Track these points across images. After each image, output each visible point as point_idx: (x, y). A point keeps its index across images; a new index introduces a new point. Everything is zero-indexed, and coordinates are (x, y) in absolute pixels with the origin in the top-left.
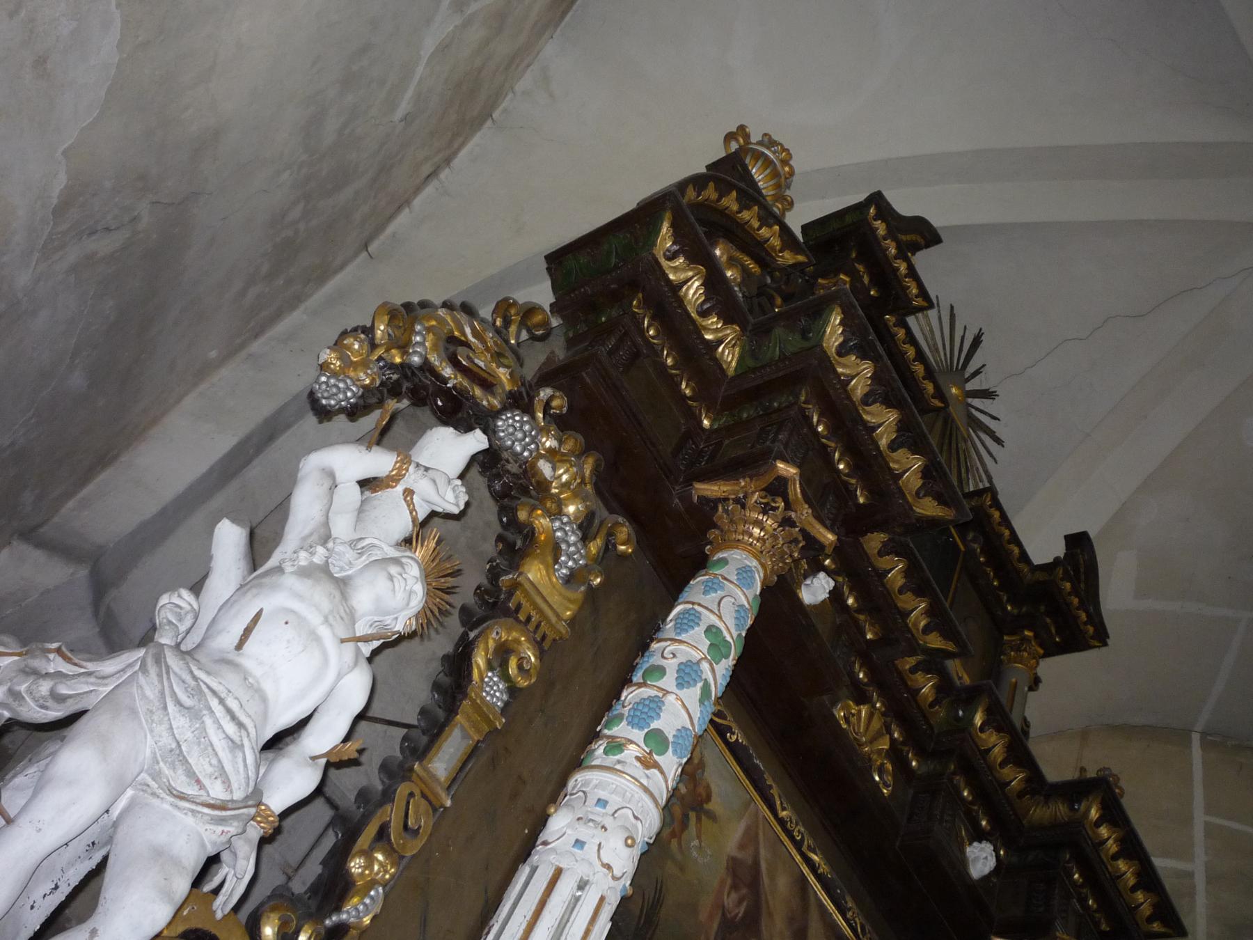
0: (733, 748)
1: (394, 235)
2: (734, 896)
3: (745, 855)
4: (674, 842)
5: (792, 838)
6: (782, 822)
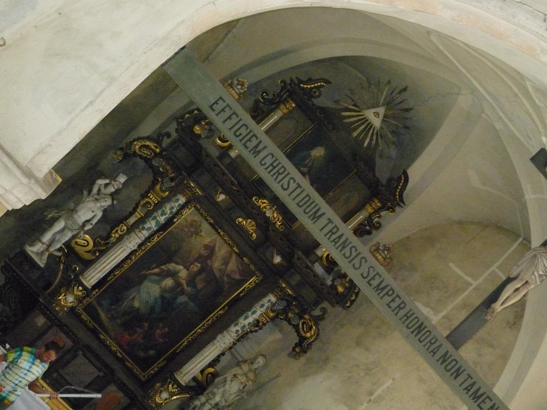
0: (210, 224)
1: (218, 52)
2: (204, 251)
3: (212, 245)
4: (187, 239)
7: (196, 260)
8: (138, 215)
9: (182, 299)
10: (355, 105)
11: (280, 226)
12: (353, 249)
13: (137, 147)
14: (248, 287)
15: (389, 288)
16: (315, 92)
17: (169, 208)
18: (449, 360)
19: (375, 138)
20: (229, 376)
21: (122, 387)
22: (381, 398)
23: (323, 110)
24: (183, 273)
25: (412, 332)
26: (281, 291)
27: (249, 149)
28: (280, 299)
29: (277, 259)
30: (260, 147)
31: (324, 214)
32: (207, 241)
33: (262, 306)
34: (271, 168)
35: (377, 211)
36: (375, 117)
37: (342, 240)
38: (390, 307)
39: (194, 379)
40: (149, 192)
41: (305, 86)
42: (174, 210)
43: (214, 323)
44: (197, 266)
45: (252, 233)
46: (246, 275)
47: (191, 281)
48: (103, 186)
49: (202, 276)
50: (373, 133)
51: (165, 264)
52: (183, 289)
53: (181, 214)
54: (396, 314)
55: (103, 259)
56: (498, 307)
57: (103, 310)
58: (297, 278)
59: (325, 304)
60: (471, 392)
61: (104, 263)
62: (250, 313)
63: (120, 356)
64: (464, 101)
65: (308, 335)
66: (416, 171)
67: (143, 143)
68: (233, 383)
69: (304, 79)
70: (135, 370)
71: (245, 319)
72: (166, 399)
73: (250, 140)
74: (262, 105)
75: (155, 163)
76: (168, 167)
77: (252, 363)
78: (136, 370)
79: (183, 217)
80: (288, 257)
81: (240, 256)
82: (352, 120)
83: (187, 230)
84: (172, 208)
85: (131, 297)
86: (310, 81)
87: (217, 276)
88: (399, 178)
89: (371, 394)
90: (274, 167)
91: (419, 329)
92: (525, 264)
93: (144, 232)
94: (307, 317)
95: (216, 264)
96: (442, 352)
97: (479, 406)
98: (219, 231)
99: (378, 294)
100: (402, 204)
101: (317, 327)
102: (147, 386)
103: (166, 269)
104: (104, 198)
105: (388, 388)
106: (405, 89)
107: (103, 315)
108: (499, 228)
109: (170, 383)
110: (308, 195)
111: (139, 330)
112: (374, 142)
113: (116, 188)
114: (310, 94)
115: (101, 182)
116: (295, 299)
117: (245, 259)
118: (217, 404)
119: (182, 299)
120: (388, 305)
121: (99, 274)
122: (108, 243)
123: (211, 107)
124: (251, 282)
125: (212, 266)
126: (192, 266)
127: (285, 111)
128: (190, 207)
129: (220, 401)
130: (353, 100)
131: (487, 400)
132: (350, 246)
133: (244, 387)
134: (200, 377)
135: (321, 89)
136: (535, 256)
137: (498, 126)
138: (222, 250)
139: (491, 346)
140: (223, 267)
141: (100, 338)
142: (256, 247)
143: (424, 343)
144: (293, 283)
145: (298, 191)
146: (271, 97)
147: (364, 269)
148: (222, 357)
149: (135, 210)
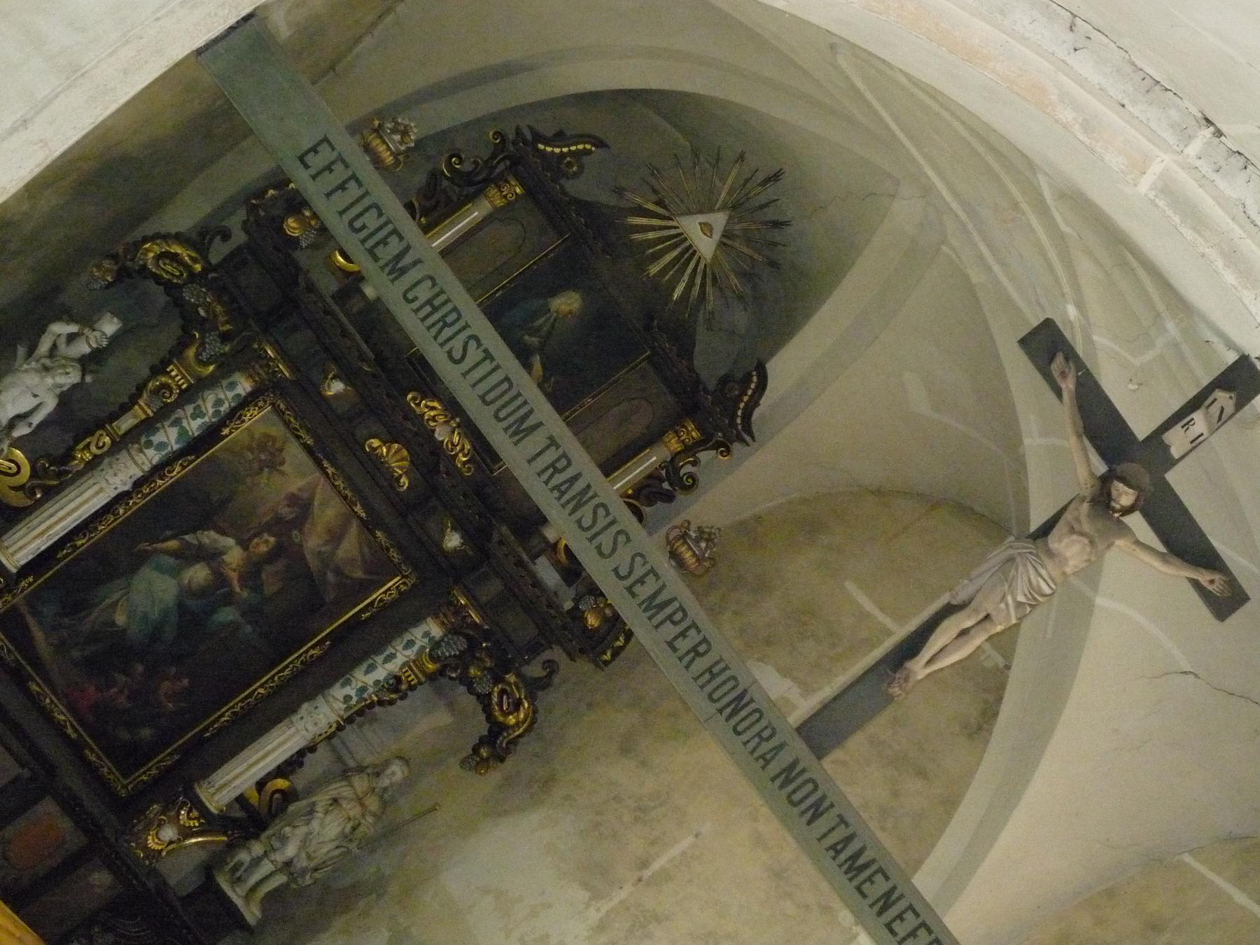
0: (306, 447)
2: (287, 510)
3: (305, 495)
4: (248, 480)
7: (268, 528)
8: (140, 412)
9: (227, 615)
10: (659, 203)
11: (464, 463)
12: (601, 512)
13: (151, 255)
14: (381, 600)
15: (676, 604)
16: (569, 165)
17: (212, 404)
18: (799, 781)
19: (698, 280)
20: (322, 799)
21: (71, 806)
22: (664, 876)
23: (586, 208)
24: (234, 556)
25: (720, 711)
26: (456, 613)
27: (382, 263)
28: (453, 631)
29: (453, 541)
30: (407, 260)
31: (540, 424)
32: (295, 484)
33: (410, 644)
34: (428, 309)
35: (690, 450)
36: (703, 234)
37: (580, 485)
38: (675, 650)
39: (241, 800)
40: (170, 362)
41: (549, 149)
42: (224, 408)
43: (297, 676)
45: (401, 476)
46: (379, 570)
47: (251, 574)
48: (63, 339)
49: (280, 565)
50: (695, 270)
51: (194, 530)
53: (239, 418)
54: (687, 667)
55: (50, 508)
56: (918, 668)
57: (40, 623)
58: (493, 588)
59: (556, 653)
60: (843, 857)
61: (51, 516)
62: (379, 659)
63: (74, 736)
64: (904, 212)
65: (512, 720)
66: (785, 368)
67: (165, 248)
68: (329, 818)
69: (548, 130)
70: (106, 770)
71: (367, 673)
72: (171, 842)
73: (384, 242)
74: (445, 183)
75: (189, 295)
76: (219, 309)
77: (378, 775)
78: (107, 769)
79: (245, 425)
80: (477, 536)
81: (368, 526)
82: (651, 235)
83: (250, 456)
84: (219, 402)
85: (108, 601)
86: (559, 137)
88: (747, 379)
89: (644, 864)
90: (435, 309)
91: (738, 707)
92: (987, 575)
93: (150, 452)
94: (511, 678)
95: (313, 542)
96: (784, 759)
97: (859, 889)
98: (326, 464)
99: (650, 618)
100: (748, 438)
101: (532, 703)
102: (131, 809)
104: (64, 366)
105: (683, 853)
106: (775, 177)
107: (38, 635)
108: (963, 510)
109: (184, 804)
110: (507, 379)
111: (121, 679)
112: (696, 290)
113: (94, 346)
114: (556, 166)
115: (61, 329)
116: (487, 635)
117: (379, 534)
118: (288, 864)
119: (227, 615)
120: (671, 644)
121: (39, 541)
122: (67, 472)
123: (301, 159)
124: (389, 589)
126: (256, 540)
127: (499, 202)
128: (260, 404)
129: (297, 856)
130: (655, 191)
131: (879, 878)
132: (595, 501)
133: (354, 829)
134: (254, 798)
135: (585, 159)
136: (1011, 559)
137: (976, 275)
138: (328, 511)
139: (922, 774)
140: (323, 549)
141: (29, 689)
142: (406, 507)
143: (745, 737)
144: (484, 599)
145: (487, 366)
146: (468, 167)
147: (623, 557)
148: (309, 755)
149: (133, 400)
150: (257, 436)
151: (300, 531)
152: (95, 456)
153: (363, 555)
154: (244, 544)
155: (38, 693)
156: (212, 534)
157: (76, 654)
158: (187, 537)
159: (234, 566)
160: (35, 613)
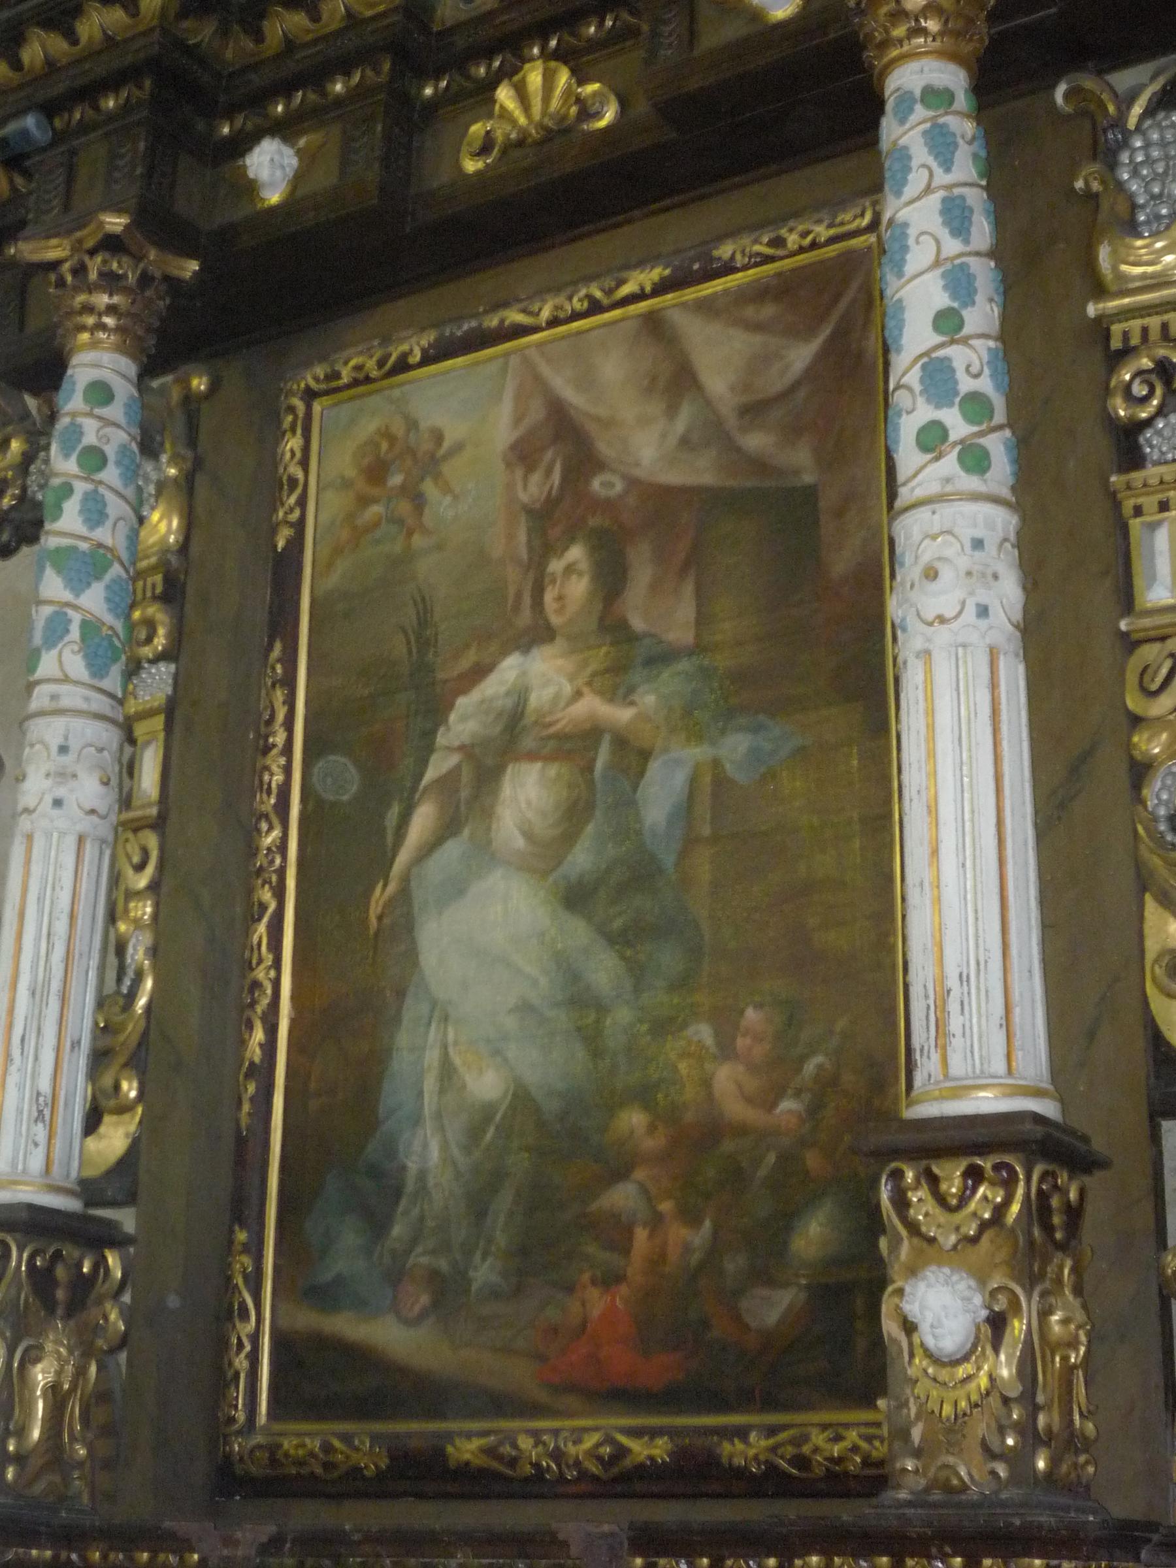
2: (536, 477)
3: (537, 412)
4: (418, 541)
5: (576, 316)
6: (554, 322)
32: (502, 429)
44: (570, 569)
45: (579, 100)
47: (623, 655)
49: (642, 572)
52: (621, 742)
57: (362, 1306)
63: (660, 1450)
70: (819, 1439)
83: (376, 509)
85: (430, 1084)
87: (708, 479)
93: (47, 665)
95: (647, 447)
103: (454, 759)
111: (622, 1197)
117: (725, 251)
125: (633, 483)
126: (549, 597)
150: (351, 473)
151: (600, 465)
152: (154, 887)
153: (757, 327)
154: (540, 634)
155: (490, 1452)
156: (463, 703)
157: (484, 1273)
158: (430, 775)
159: (568, 689)
160: (324, 1296)
